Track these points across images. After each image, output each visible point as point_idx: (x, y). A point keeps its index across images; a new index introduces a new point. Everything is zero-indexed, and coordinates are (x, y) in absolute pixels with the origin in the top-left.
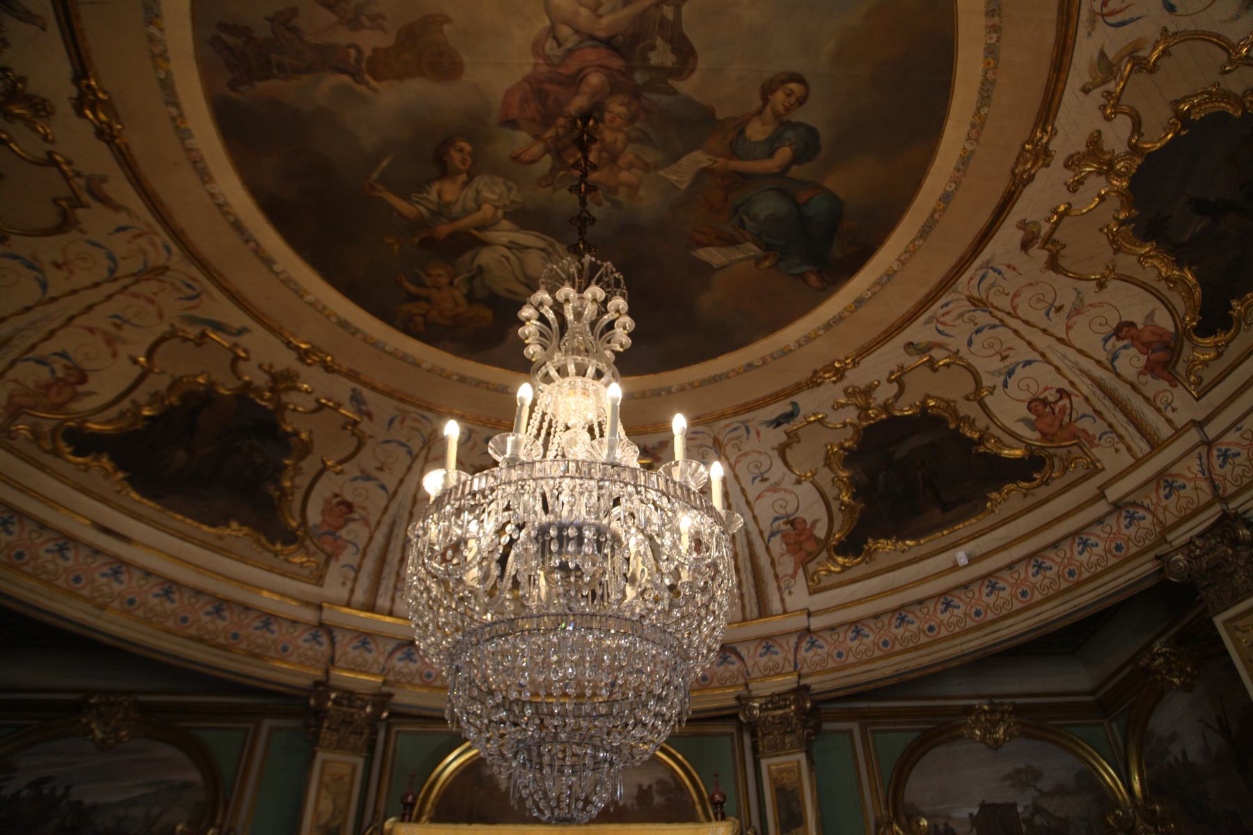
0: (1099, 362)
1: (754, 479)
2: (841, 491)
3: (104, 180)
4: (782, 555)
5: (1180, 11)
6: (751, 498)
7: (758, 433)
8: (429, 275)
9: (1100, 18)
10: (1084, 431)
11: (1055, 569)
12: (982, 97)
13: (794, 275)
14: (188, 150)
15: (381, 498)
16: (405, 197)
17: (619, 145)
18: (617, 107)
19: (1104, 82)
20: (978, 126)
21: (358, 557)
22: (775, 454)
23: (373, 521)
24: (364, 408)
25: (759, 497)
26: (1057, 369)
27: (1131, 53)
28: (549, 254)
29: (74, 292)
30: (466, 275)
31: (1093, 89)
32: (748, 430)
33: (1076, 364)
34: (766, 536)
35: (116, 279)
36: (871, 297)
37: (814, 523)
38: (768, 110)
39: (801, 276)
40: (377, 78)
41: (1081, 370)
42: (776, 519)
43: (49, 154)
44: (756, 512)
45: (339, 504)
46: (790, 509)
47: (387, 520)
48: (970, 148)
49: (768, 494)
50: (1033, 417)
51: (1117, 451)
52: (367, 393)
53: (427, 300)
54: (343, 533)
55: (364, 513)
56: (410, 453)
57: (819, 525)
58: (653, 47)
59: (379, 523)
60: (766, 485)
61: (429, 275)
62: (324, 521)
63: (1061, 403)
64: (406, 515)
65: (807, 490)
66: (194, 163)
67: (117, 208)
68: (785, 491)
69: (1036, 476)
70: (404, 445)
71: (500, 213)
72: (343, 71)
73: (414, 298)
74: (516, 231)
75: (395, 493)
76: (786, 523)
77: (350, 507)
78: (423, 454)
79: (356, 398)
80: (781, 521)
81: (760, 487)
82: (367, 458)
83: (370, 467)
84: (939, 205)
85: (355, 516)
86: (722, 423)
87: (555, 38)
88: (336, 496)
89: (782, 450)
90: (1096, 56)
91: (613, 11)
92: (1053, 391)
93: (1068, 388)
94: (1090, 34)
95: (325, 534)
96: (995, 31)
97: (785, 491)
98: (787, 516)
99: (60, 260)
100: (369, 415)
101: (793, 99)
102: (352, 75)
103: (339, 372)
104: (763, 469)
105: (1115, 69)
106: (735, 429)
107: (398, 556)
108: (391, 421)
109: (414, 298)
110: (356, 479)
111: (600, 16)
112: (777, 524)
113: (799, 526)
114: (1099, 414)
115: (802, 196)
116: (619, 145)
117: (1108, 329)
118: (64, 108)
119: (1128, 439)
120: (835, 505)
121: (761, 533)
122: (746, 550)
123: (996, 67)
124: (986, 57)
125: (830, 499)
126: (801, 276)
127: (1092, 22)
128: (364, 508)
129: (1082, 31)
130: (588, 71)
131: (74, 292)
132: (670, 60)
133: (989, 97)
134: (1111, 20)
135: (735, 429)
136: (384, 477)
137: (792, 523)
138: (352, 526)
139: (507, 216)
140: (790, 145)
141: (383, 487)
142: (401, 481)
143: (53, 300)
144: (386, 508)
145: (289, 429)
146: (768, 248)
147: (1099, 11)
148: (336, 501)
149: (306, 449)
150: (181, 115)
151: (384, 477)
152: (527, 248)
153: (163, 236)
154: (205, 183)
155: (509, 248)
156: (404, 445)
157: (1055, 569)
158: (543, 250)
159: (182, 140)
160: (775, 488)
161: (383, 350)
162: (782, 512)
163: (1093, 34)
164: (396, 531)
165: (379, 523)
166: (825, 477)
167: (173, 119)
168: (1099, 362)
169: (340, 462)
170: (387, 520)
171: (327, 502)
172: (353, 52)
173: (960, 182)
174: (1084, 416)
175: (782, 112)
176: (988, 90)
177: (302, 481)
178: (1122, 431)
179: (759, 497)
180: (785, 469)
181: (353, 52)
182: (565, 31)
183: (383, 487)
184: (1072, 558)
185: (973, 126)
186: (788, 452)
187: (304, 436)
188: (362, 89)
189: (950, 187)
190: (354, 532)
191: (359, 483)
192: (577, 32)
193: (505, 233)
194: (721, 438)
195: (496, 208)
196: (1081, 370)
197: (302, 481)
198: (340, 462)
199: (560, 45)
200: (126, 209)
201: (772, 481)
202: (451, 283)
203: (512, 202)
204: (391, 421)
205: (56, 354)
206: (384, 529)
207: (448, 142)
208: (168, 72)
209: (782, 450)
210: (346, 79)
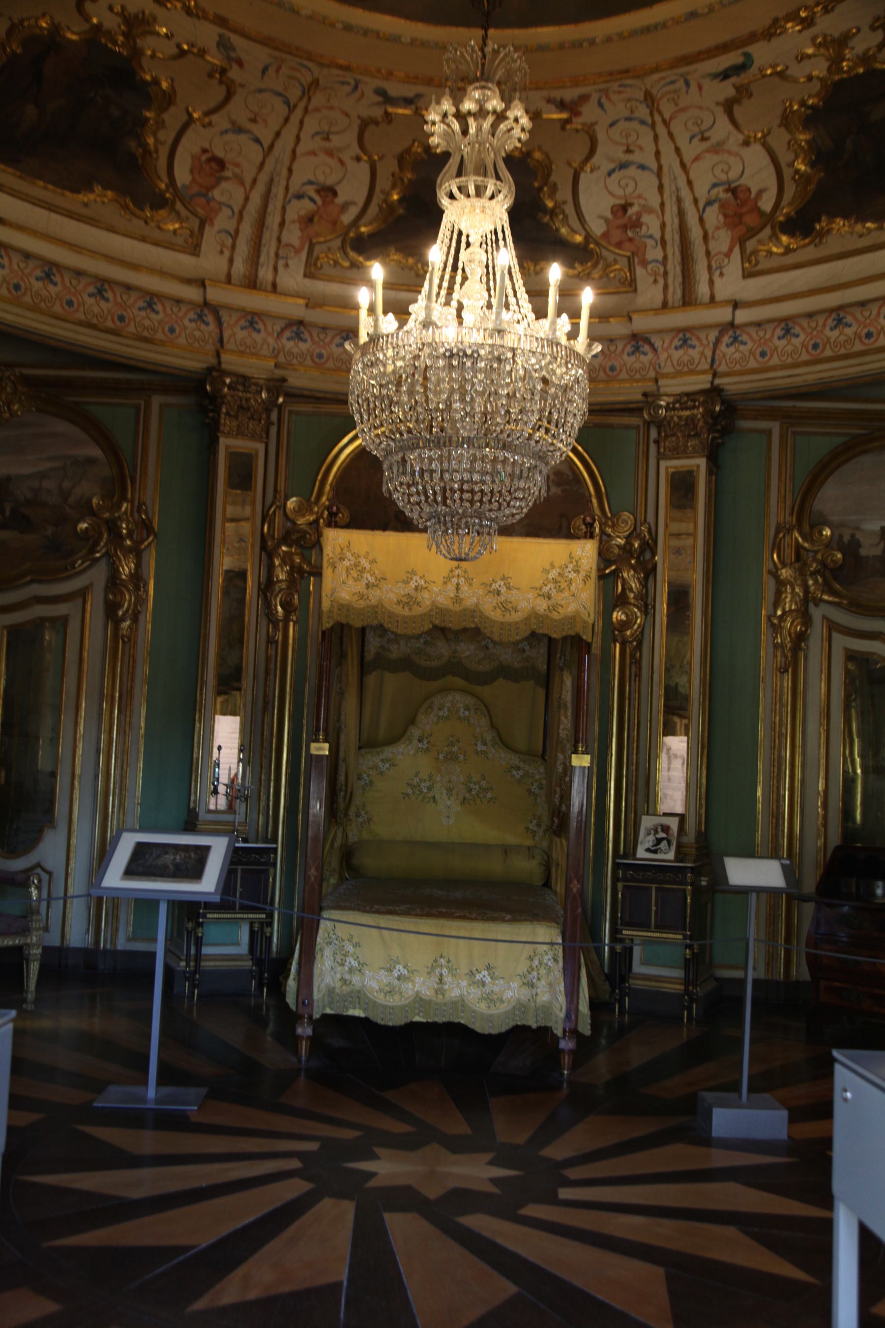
1: (692, 138)
2: (796, 158)
6: (687, 160)
7: (700, 88)
15: (255, 153)
22: (720, 111)
23: (248, 179)
24: (233, 55)
25: (697, 159)
32: (687, 84)
34: (701, 205)
37: (760, 192)
42: (715, 185)
44: (692, 176)
45: (209, 160)
46: (733, 174)
47: (263, 178)
49: (708, 156)
55: (237, 170)
56: (287, 102)
57: (765, 196)
59: (254, 181)
60: (705, 145)
62: (194, 179)
64: (285, 172)
65: (756, 156)
68: (729, 153)
70: (279, 94)
75: (271, 147)
77: (221, 164)
78: (302, 105)
80: (721, 189)
81: (698, 147)
82: (237, 109)
83: (242, 119)
86: (655, 77)
88: (205, 151)
89: (729, 107)
97: (729, 153)
98: (729, 182)
100: (240, 63)
103: (206, 18)
104: (703, 128)
106: (673, 82)
107: (277, 219)
108: (265, 70)
110: (226, 131)
112: (715, 191)
113: (741, 195)
120: (787, 173)
121: (696, 201)
122: (676, 221)
125: (783, 164)
128: (237, 165)
135: (673, 82)
136: (258, 130)
137: (734, 191)
141: (257, 141)
142: (278, 134)
144: (262, 164)
148: (204, 158)
149: (169, 99)
151: (258, 130)
156: (279, 94)
160: (717, 149)
162: (723, 177)
164: (274, 190)
165: (254, 181)
166: (780, 140)
169: (207, 114)
170: (263, 178)
171: (194, 158)
177: (167, 136)
179: (697, 159)
180: (730, 127)
183: (257, 141)
186: (736, 108)
187: (164, 85)
191: (230, 137)
194: (654, 91)
197: (167, 136)
198: (207, 114)
201: (713, 141)
204: (265, 70)
209: (729, 107)
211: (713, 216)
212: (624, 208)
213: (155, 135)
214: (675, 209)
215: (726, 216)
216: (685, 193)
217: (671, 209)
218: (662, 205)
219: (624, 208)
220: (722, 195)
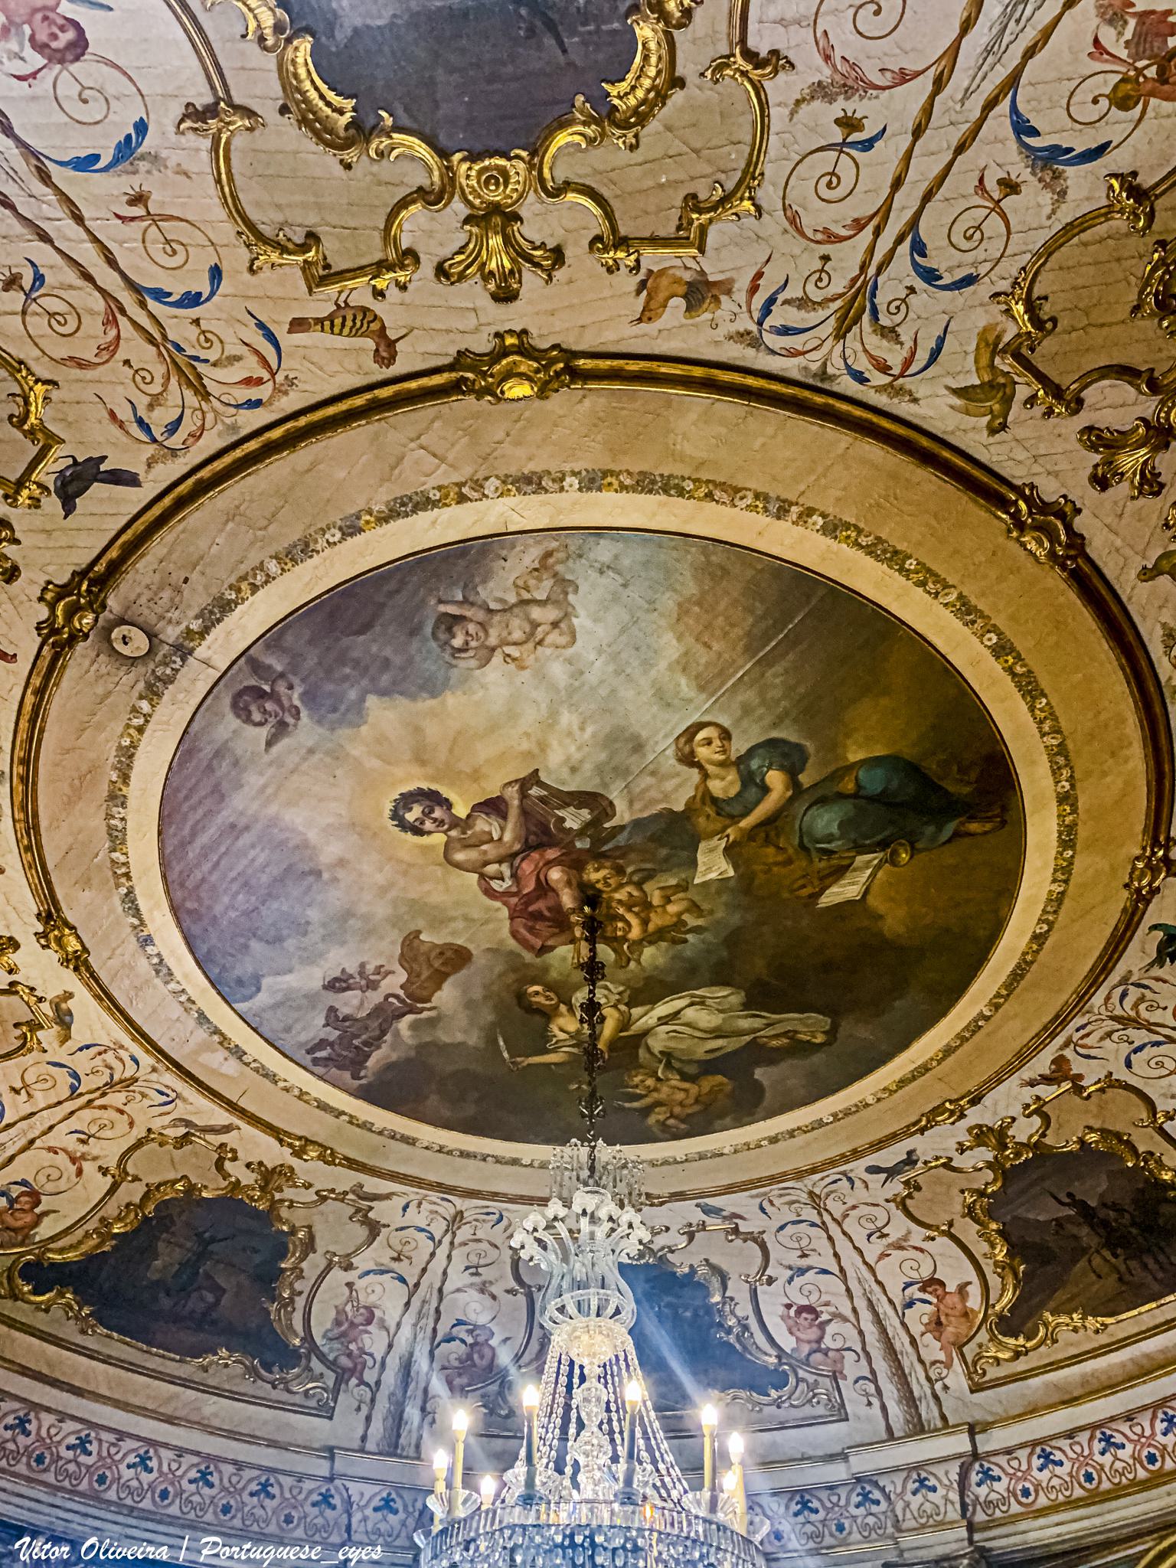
3: (361, 1186)
5: (983, 269)
8: (637, 1086)
9: (901, 381)
12: (889, 561)
13: (949, 841)
14: (381, 1133)
16: (547, 1052)
17: (635, 893)
18: (594, 875)
19: (1007, 401)
20: (928, 579)
21: (864, 1362)
27: (994, 353)
28: (702, 1003)
29: (424, 1270)
30: (662, 1066)
31: (1005, 419)
35: (440, 1242)
36: (1073, 786)
38: (711, 769)
39: (957, 835)
40: (428, 1000)
43: (317, 1193)
48: (952, 597)
52: (709, 1201)
53: (658, 1104)
54: (828, 1342)
58: (562, 820)
61: (637, 1086)
66: (393, 1137)
67: (388, 1197)
71: (622, 1007)
72: (404, 1015)
73: (647, 1111)
74: (652, 1009)
79: (708, 1211)
83: (793, 1258)
84: (1006, 661)
85: (825, 1317)
87: (492, 878)
90: (958, 402)
91: (502, 829)
94: (915, 400)
95: (809, 1355)
96: (810, 515)
99: (395, 1255)
101: (717, 742)
102: (410, 1012)
105: (1002, 380)
109: (647, 1111)
111: (500, 839)
115: (849, 786)
116: (635, 893)
118: (294, 1162)
123: (859, 531)
124: (836, 538)
126: (957, 835)
127: (900, 392)
129: (903, 408)
130: (542, 877)
131: (424, 1270)
132: (586, 814)
133: (896, 552)
134: (913, 369)
138: (830, 1329)
139: (629, 1005)
140: (769, 768)
143: (417, 1285)
145: (686, 1270)
146: (883, 845)
147: (891, 378)
150: (351, 1116)
152: (678, 1012)
153: (434, 1196)
154: (414, 1144)
155: (666, 1024)
158: (692, 1004)
159: (370, 1130)
161: (676, 1162)
163: (917, 396)
167: (350, 1122)
172: (391, 1000)
173: (994, 626)
175: (722, 757)
176: (885, 551)
181: (391, 1000)
182: (491, 869)
185: (922, 584)
188: (425, 1015)
189: (990, 639)
190: (838, 1334)
192: (500, 862)
193: (647, 1017)
195: (615, 1006)
197: (745, 1309)
199: (503, 879)
200: (393, 1194)
202: (659, 1079)
203: (620, 994)
205: (454, 1326)
206: (866, 1316)
207: (521, 997)
208: (315, 1100)
210: (409, 1018)
213: (732, 1312)
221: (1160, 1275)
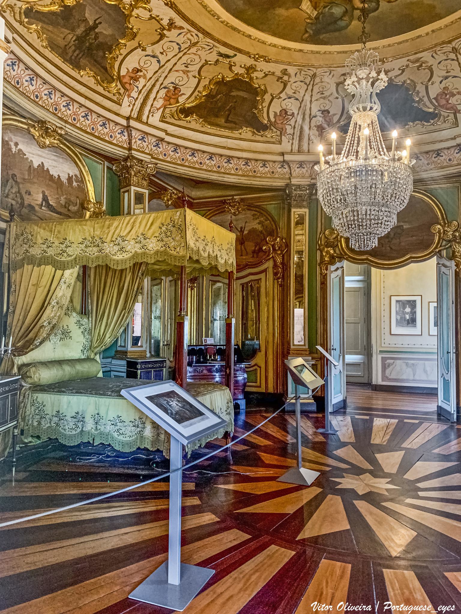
0: (310, 114)
4: (161, 98)
10: (286, 129)
11: (251, 167)
26: (300, 107)
33: (305, 110)
41: (304, 113)
50: (279, 114)
51: (289, 142)
57: (183, 96)
63: (289, 116)
69: (261, 131)
76: (173, 87)
80: (173, 85)
92: (291, 112)
93: (296, 115)
113: (176, 92)
114: (294, 127)
117: (323, 109)
119: (294, 141)
121: (162, 84)
137: (175, 88)
157: (251, 167)
168: (310, 114)
174: (290, 125)
178: (295, 137)
184: (257, 167)
196: (304, 113)
211: (162, 93)
212: (138, 71)
214: (153, 82)
215: (166, 95)
216: (161, 80)
217: (152, 81)
218: (151, 78)
219: (138, 71)
220: (171, 88)
221: (73, 58)
